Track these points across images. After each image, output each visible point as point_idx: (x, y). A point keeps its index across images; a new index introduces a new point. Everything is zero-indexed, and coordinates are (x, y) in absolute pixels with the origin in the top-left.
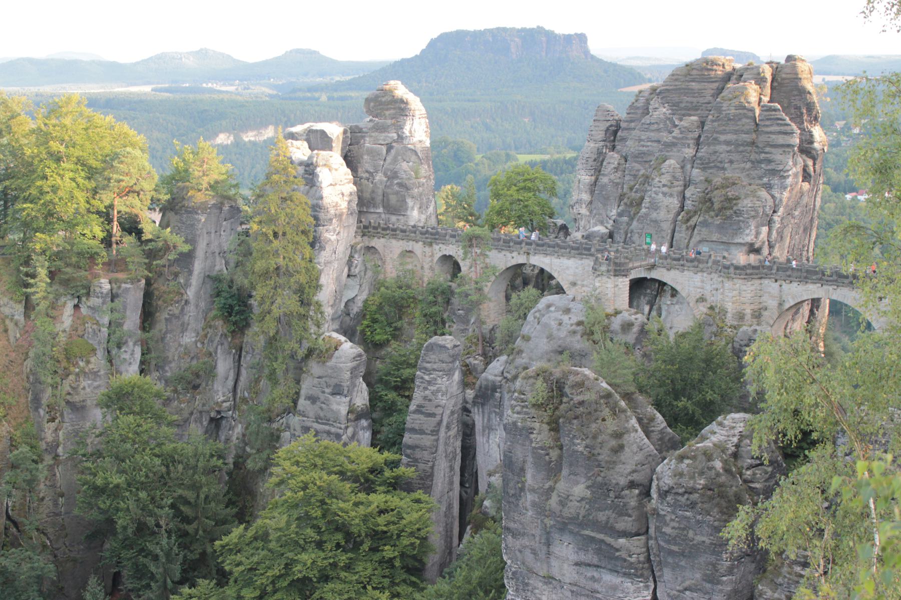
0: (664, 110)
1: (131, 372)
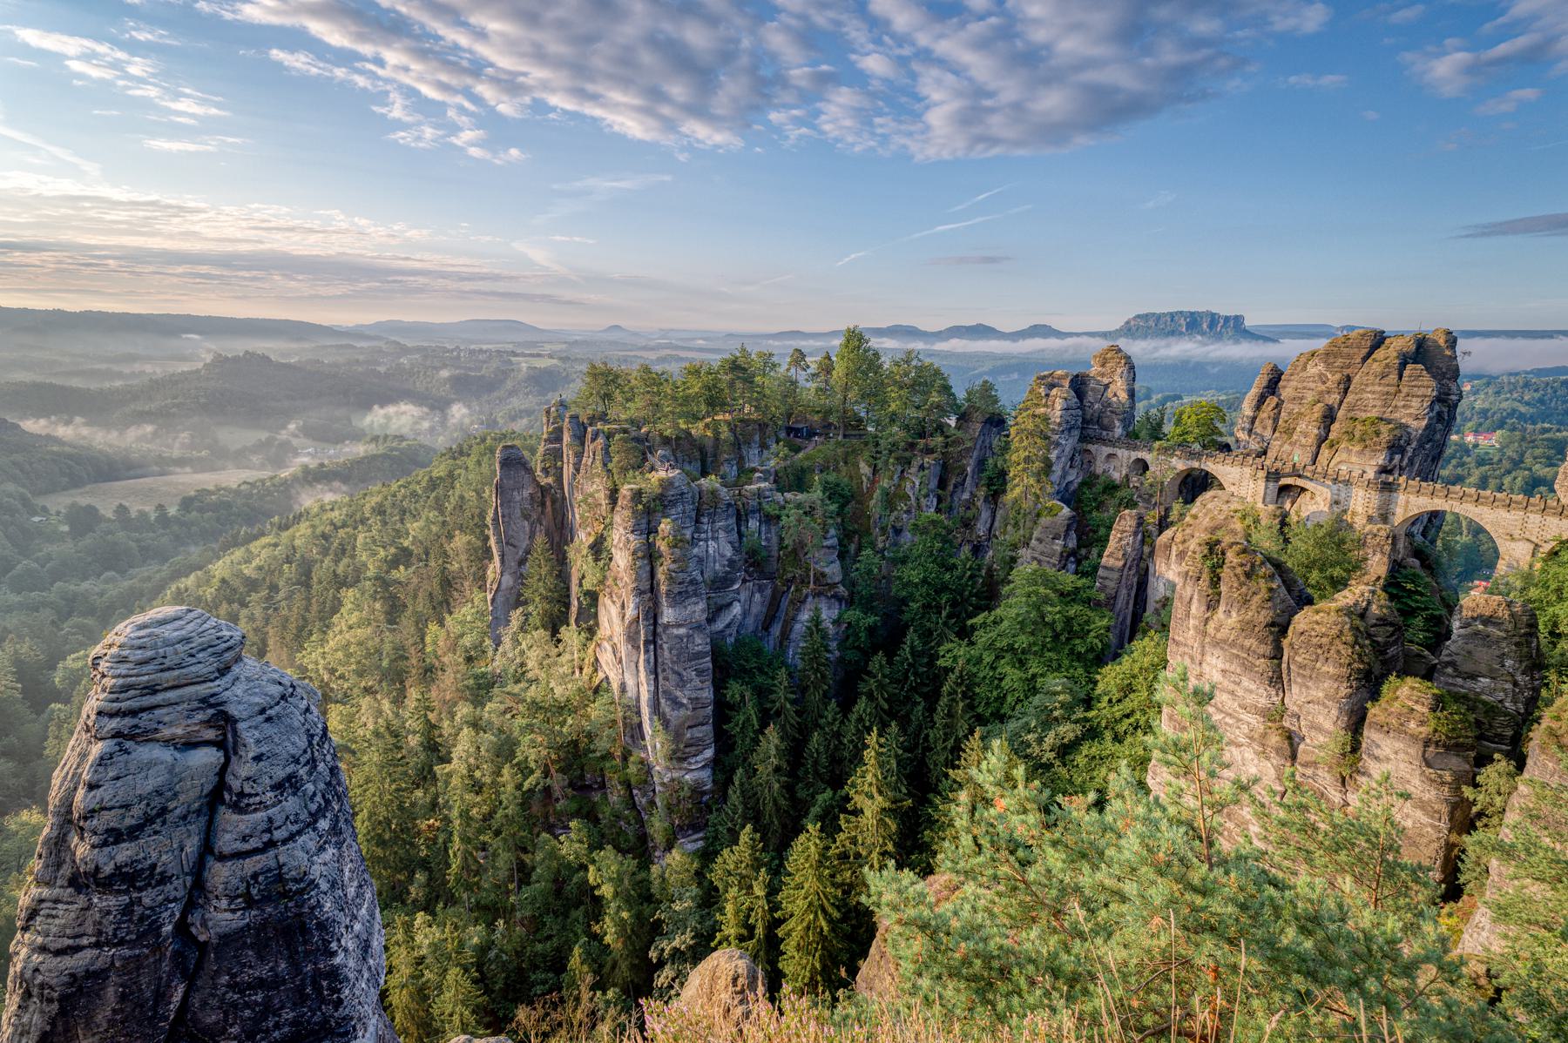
0: (1321, 367)
1: (931, 513)
